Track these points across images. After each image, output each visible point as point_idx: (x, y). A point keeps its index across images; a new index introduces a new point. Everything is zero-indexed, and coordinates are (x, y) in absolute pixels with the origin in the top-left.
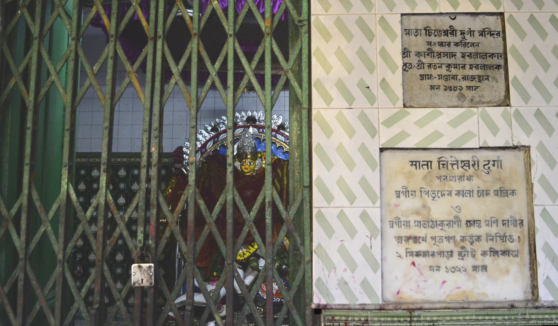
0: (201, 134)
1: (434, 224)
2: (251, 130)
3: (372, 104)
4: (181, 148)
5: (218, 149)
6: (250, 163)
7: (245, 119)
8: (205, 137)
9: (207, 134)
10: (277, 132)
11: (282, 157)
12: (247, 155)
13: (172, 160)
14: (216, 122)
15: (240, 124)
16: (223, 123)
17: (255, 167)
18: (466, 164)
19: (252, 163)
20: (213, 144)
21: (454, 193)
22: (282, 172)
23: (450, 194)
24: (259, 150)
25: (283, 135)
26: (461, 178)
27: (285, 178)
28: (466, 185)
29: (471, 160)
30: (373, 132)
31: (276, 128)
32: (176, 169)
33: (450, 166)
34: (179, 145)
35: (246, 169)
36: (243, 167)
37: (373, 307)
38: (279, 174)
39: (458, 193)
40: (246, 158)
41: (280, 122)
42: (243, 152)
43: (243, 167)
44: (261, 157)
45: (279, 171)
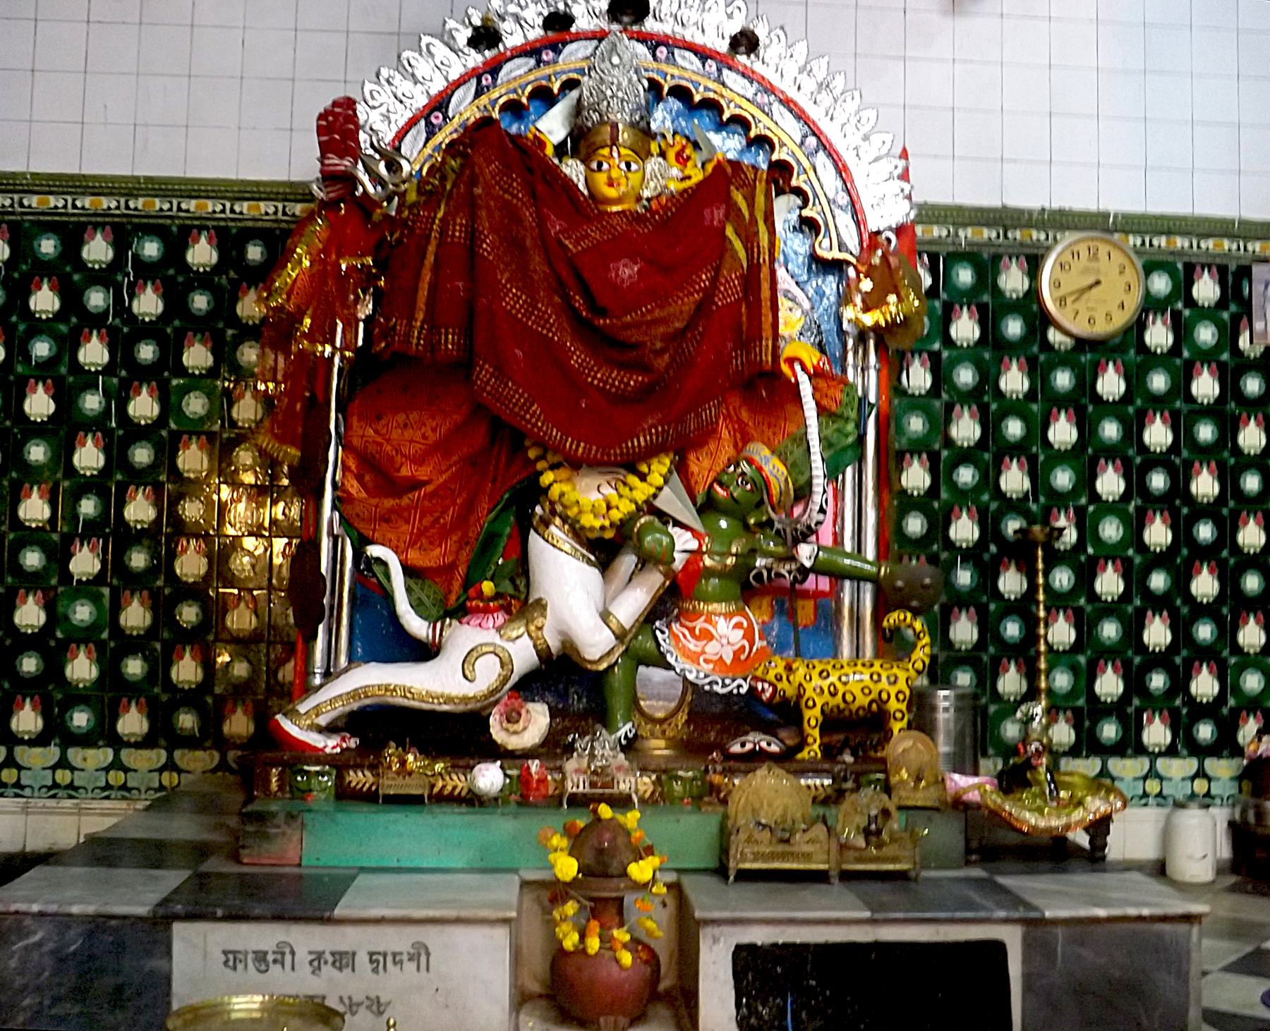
4: (350, 103)
5: (496, 115)
6: (628, 165)
10: (725, 62)
12: (615, 126)
16: (517, 18)
19: (634, 167)
20: (478, 94)
22: (751, 206)
24: (654, 126)
25: (748, 75)
27: (762, 227)
31: (723, 46)
34: (339, 93)
35: (611, 184)
36: (601, 178)
38: (740, 210)
40: (614, 141)
41: (734, 28)
42: (602, 122)
43: (601, 178)
44: (663, 154)
45: (739, 198)
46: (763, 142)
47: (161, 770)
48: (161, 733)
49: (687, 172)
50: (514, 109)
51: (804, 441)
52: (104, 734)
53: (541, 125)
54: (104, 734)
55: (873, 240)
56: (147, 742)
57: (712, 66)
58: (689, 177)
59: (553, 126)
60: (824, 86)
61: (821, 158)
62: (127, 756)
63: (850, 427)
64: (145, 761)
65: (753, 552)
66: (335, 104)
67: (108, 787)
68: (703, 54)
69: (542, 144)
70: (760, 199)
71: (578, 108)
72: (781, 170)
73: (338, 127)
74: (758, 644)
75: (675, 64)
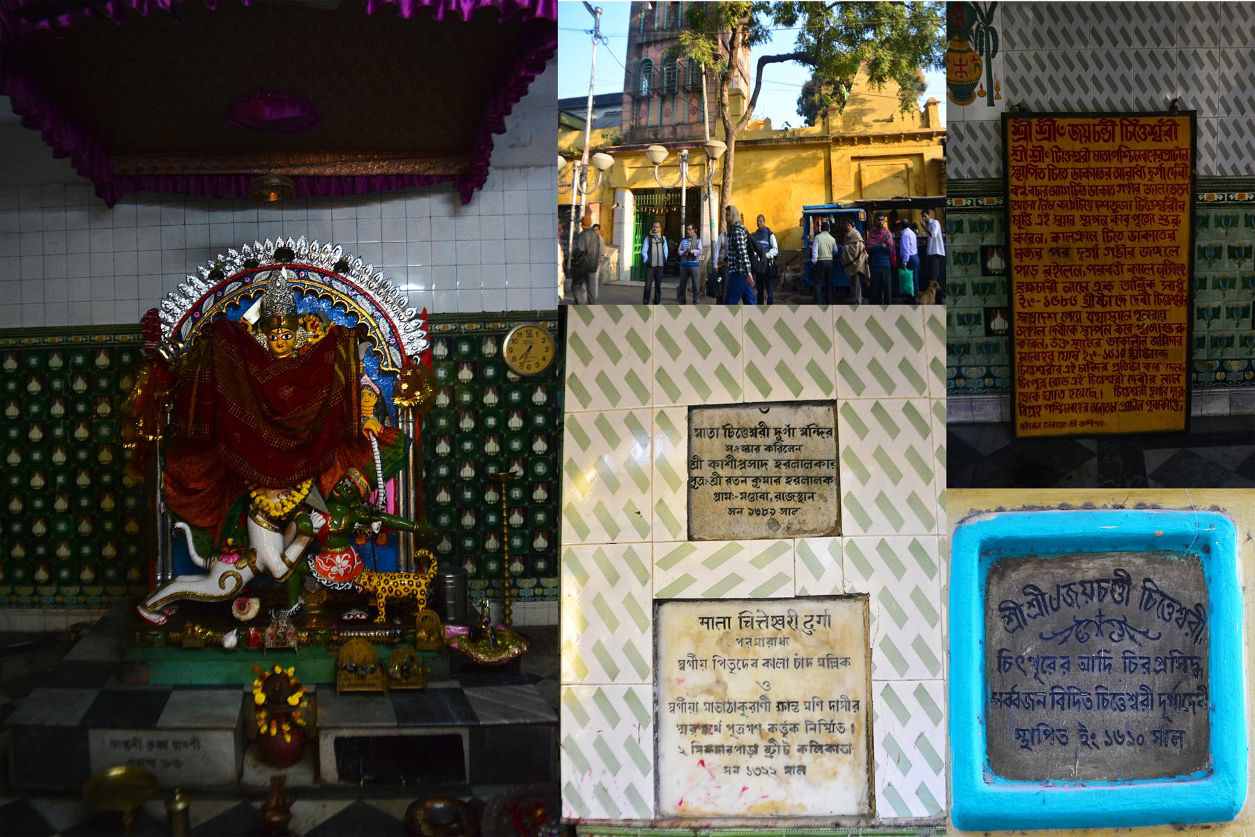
0: (191, 284)
1: (731, 707)
2: (284, 272)
3: (643, 537)
4: (155, 312)
7: (272, 253)
8: (199, 290)
9: (202, 285)
10: (333, 275)
11: (342, 322)
13: (141, 336)
14: (218, 261)
15: (263, 262)
16: (232, 263)
17: (295, 342)
18: (779, 620)
20: (215, 302)
21: (760, 662)
23: (755, 664)
25: (344, 281)
26: (772, 641)
28: (778, 651)
29: (786, 615)
30: (645, 577)
32: (148, 351)
33: (756, 624)
37: (641, 824)
39: (767, 663)
41: (337, 258)
44: (304, 326)
46: (353, 314)
47: (101, 595)
48: (99, 580)
49: (318, 332)
50: (233, 305)
51: (375, 472)
52: (75, 580)
53: (245, 316)
54: (75, 580)
55: (407, 361)
56: (94, 583)
57: (327, 279)
58: (317, 336)
59: (252, 315)
60: (383, 285)
61: (382, 322)
62: (87, 589)
63: (401, 451)
64: (95, 591)
65: (353, 525)
66: (149, 313)
67: (78, 603)
68: (323, 273)
69: (247, 326)
70: (352, 347)
71: (262, 310)
72: (362, 329)
73: (152, 321)
74: (357, 563)
75: (309, 279)
